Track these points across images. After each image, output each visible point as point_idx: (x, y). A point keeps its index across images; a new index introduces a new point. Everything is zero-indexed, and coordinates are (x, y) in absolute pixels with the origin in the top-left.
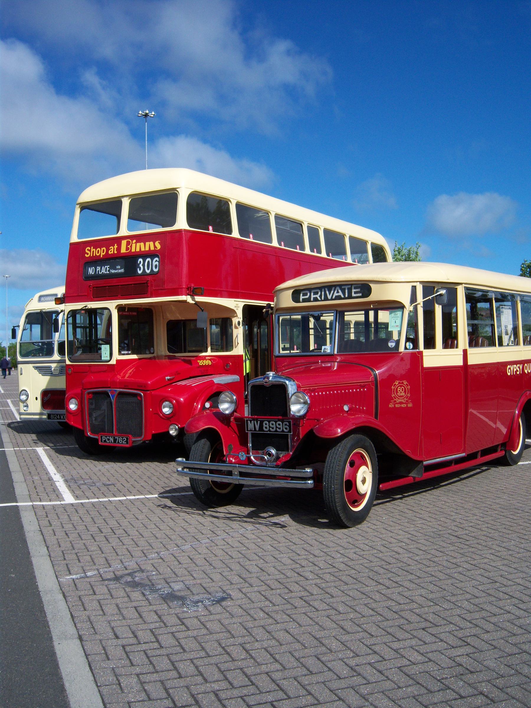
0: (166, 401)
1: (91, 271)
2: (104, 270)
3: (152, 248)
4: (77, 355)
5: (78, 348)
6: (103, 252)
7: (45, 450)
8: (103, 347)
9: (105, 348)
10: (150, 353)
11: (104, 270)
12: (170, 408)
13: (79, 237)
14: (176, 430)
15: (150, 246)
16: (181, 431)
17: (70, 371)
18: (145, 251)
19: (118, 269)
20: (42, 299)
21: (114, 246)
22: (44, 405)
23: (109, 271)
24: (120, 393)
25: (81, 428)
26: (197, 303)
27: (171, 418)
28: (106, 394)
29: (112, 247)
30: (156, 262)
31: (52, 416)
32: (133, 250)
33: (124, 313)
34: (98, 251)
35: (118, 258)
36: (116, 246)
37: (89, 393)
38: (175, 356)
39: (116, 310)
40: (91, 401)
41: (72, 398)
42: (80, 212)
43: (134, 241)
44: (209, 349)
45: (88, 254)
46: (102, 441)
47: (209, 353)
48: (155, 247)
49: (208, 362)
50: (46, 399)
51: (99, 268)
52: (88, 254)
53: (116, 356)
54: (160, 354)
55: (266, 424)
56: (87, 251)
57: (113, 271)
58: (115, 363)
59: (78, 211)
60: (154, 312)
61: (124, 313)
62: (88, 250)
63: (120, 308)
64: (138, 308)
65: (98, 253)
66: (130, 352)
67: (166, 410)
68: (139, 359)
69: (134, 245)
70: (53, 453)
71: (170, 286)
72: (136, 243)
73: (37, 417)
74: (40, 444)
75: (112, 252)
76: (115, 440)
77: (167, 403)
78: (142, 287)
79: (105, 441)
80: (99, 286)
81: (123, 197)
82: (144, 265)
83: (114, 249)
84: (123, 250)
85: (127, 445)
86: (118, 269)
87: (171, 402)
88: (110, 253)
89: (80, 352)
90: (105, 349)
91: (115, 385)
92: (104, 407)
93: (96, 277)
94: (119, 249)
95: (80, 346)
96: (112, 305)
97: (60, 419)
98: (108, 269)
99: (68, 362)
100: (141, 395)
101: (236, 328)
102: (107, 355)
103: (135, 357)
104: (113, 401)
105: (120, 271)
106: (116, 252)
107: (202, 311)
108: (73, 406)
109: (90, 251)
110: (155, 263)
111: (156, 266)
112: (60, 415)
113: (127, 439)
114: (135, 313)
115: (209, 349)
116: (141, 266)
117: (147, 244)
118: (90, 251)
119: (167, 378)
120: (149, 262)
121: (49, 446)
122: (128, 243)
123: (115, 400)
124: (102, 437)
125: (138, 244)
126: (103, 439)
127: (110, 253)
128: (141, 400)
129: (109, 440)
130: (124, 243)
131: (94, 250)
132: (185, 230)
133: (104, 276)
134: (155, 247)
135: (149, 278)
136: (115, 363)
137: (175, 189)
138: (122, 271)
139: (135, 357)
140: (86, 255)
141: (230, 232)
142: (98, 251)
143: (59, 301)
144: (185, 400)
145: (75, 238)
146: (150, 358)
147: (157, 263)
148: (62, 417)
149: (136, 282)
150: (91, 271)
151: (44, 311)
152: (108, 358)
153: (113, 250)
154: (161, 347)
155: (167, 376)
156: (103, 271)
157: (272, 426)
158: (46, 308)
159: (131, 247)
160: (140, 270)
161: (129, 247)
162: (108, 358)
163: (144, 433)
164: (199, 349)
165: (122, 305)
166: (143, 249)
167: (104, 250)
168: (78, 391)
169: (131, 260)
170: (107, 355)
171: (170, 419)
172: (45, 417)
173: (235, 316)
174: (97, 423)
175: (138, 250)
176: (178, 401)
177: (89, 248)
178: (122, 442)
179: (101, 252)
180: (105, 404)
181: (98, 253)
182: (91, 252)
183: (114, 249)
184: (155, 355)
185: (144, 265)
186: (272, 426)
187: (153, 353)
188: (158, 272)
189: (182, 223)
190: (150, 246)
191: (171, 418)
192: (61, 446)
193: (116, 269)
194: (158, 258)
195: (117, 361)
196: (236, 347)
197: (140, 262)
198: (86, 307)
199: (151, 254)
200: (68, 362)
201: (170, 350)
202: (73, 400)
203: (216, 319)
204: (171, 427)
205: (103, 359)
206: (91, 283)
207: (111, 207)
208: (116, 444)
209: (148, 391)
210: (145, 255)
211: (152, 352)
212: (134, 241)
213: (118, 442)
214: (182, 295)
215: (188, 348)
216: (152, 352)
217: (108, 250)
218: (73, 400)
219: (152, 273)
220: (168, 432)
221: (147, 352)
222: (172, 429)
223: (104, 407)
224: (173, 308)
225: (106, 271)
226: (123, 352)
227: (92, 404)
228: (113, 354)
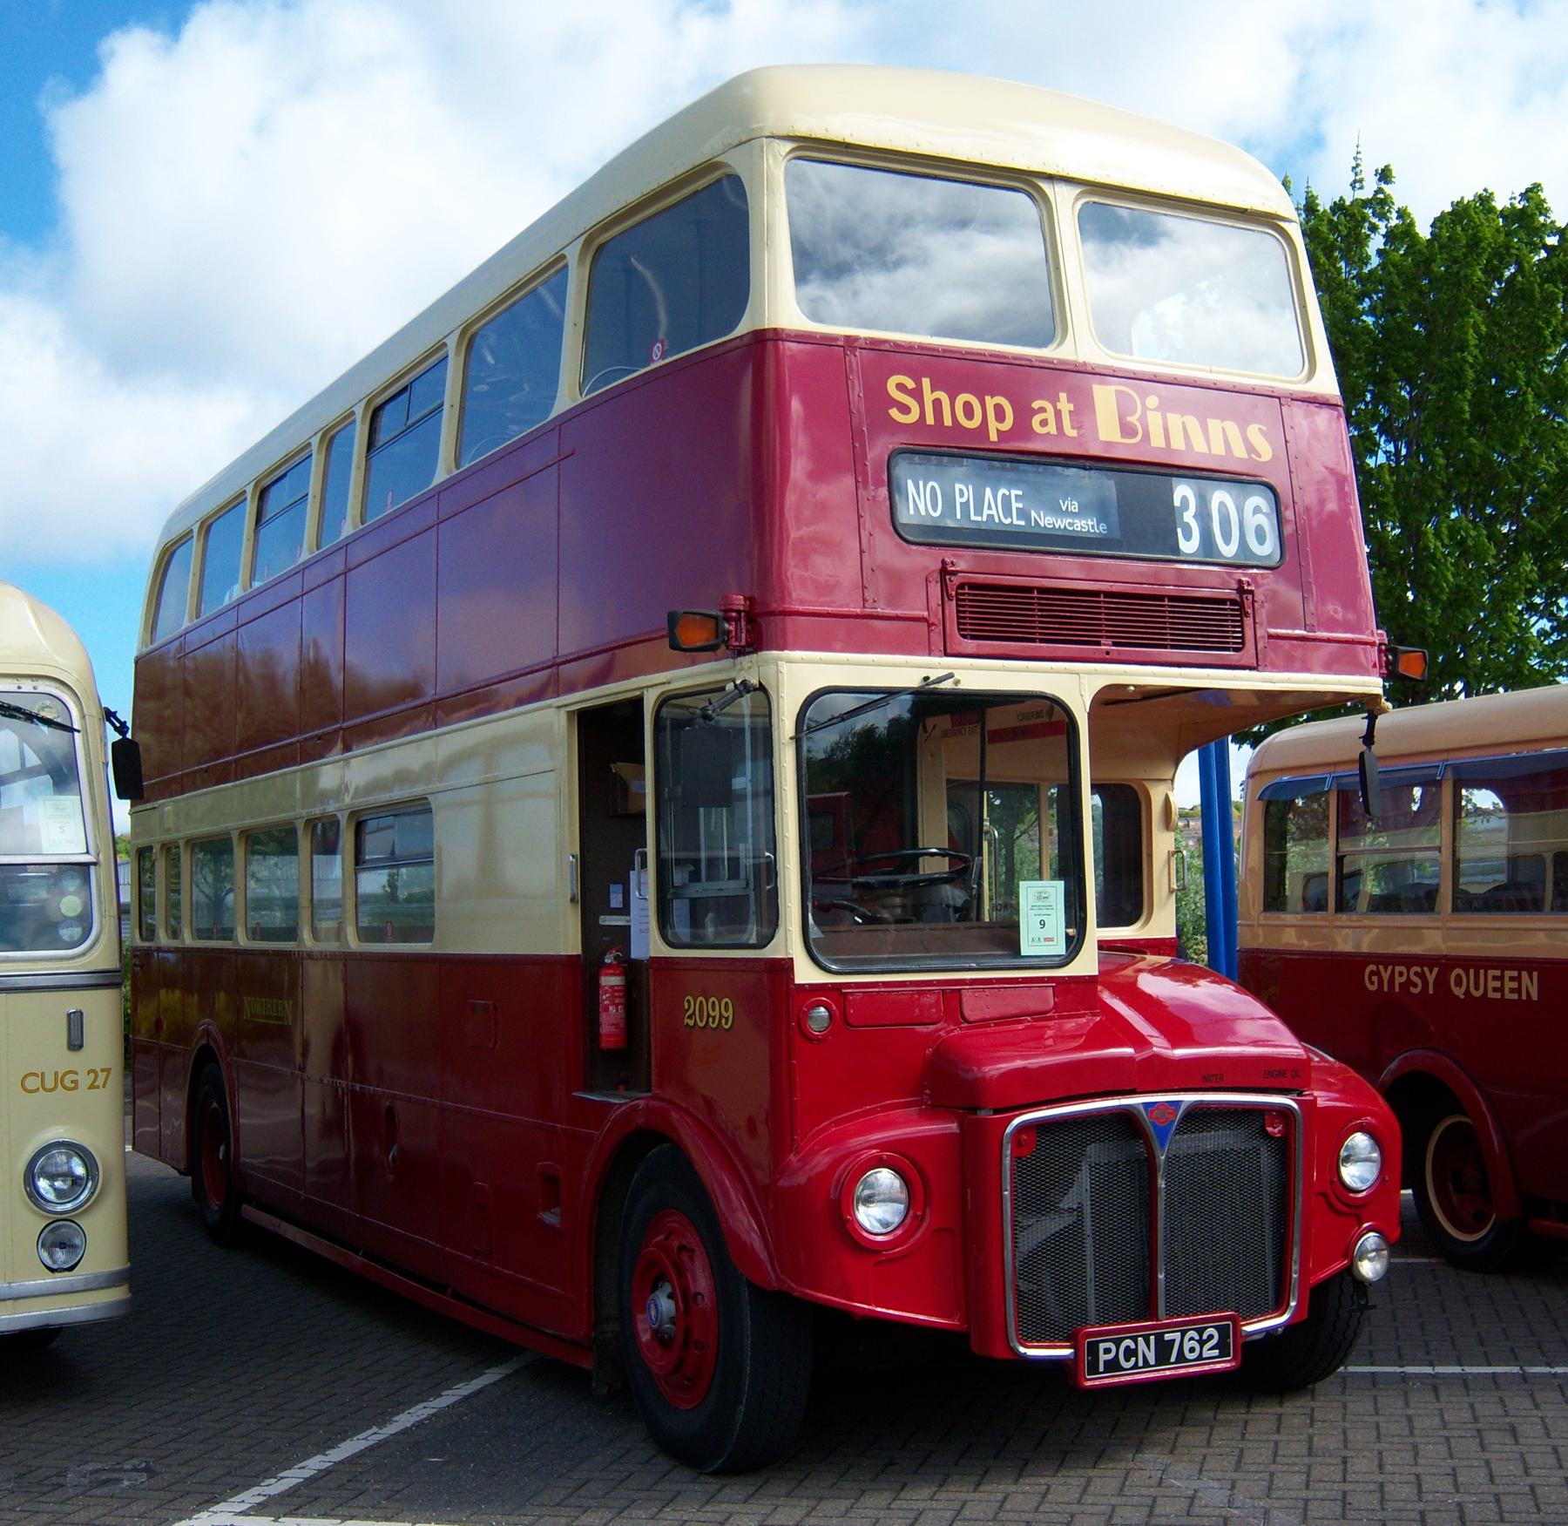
9: (1041, 897)
19: (1068, 513)
21: (1054, 401)
23: (1022, 514)
46: (1094, 1369)
52: (905, 409)
62: (901, 387)
76: (1163, 1351)
78: (1213, 621)
79: (1113, 1365)
80: (980, 578)
83: (1058, 414)
86: (1068, 513)
98: (1015, 505)
109: (917, 394)
116: (1189, 517)
118: (917, 394)
124: (1094, 1349)
126: (1103, 1357)
134: (1250, 448)
152: (1060, 948)
160: (1188, 537)
183: (1058, 414)
193: (1057, 511)
197: (1184, 500)
205: (1025, 950)
213: (1181, 1357)
225: (1007, 511)
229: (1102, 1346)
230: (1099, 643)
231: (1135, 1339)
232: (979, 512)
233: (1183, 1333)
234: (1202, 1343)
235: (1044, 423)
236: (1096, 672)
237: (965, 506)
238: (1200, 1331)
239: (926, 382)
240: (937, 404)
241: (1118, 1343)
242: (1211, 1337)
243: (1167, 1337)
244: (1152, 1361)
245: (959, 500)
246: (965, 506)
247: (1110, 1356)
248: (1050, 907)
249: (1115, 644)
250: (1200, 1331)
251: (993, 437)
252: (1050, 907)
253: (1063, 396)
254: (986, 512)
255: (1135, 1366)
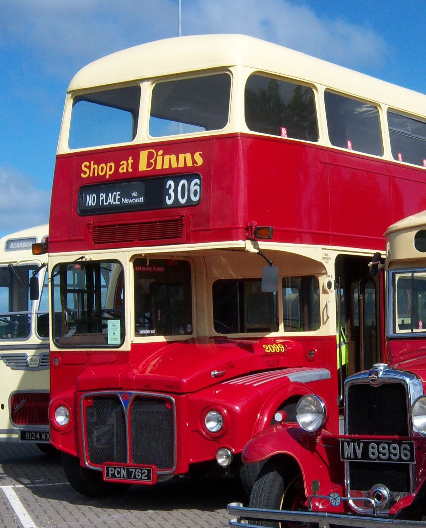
0: (212, 410)
1: (90, 200)
2: (112, 199)
3: (190, 164)
4: (68, 335)
5: (70, 325)
6: (110, 170)
7: (17, 490)
8: (110, 323)
9: (114, 325)
10: (187, 333)
11: (112, 199)
12: (218, 421)
13: (71, 146)
14: (228, 457)
15: (185, 160)
16: (236, 460)
17: (56, 363)
18: (178, 168)
19: (135, 197)
20: (12, 245)
21: (127, 160)
22: (15, 416)
23: (120, 200)
24: (138, 398)
25: (74, 453)
26: (262, 253)
27: (219, 437)
28: (115, 399)
29: (125, 162)
30: (195, 185)
31: (27, 435)
32: (159, 167)
33: (144, 269)
34: (102, 168)
35: (134, 179)
36: (131, 161)
37: (87, 398)
38: (226, 338)
39: (132, 264)
40: (90, 410)
41: (60, 405)
42: (74, 105)
43: (161, 152)
44: (281, 326)
45: (85, 173)
46: (108, 475)
47: (281, 332)
48: (194, 161)
49: (279, 348)
50: (17, 407)
51: (103, 196)
52: (85, 173)
53: (132, 338)
54: (201, 334)
55: (373, 449)
56: (84, 168)
57: (126, 201)
58: (129, 349)
59: (69, 103)
60: (192, 267)
61: (144, 269)
62: (86, 166)
63: (137, 261)
64: (166, 260)
65: (102, 171)
66: (153, 332)
67: (212, 426)
68: (168, 343)
69: (160, 159)
70: (29, 494)
71: (218, 224)
72: (163, 155)
73: (4, 436)
74: (8, 479)
75: (125, 170)
76: (129, 474)
77: (213, 413)
78: (173, 225)
81: (143, 80)
82: (175, 191)
83: (128, 164)
84: (143, 167)
85: (150, 482)
86: (135, 197)
87: (220, 412)
88: (121, 171)
89: (72, 332)
90: (113, 326)
91: (129, 384)
92: (112, 420)
93: (99, 210)
94: (136, 165)
95: (73, 321)
96: (124, 256)
97: (41, 439)
98: (118, 197)
99: (53, 348)
100: (171, 401)
101: (325, 292)
102: (116, 336)
103: (161, 339)
104: (126, 410)
105: (137, 200)
106: (130, 170)
107: (271, 264)
108: (61, 419)
109: (89, 168)
110: (193, 188)
111: (196, 192)
112: (40, 433)
113: (149, 471)
114: (161, 269)
115: (281, 326)
116: (171, 192)
117: (182, 156)
118: (89, 168)
119: (213, 373)
120: (183, 186)
121: (22, 483)
122: (150, 156)
123: (130, 409)
124: (108, 468)
125: (167, 157)
126: (110, 472)
127: (121, 171)
128: (172, 409)
129: (119, 473)
130: (144, 155)
131: (96, 166)
132: (242, 135)
133: (111, 209)
134: (194, 161)
135: (185, 212)
136: (129, 349)
137: (226, 68)
138: (141, 200)
139: (161, 339)
140: (83, 175)
141: (315, 136)
142: (102, 168)
143: (39, 249)
144: (242, 409)
145: (64, 148)
146: (186, 342)
147: (197, 188)
148: (44, 437)
149: (163, 219)
150: (90, 200)
151: (14, 264)
152: (119, 342)
153: (126, 167)
154: (204, 324)
155: (213, 370)
156: (111, 200)
157: (382, 451)
158: (18, 260)
159: (155, 161)
160: (170, 199)
161: (152, 161)
162: (119, 342)
163: (175, 463)
164: (264, 326)
165: (141, 255)
166: (174, 165)
167: (111, 167)
168: (70, 394)
169: (154, 182)
170: (116, 336)
171: (218, 440)
172: (16, 436)
173: (324, 274)
174: (100, 447)
175: (166, 166)
176: (231, 411)
177: (88, 164)
178: (140, 477)
179: (106, 170)
180: (114, 415)
181: (102, 171)
182: (89, 170)
183: (128, 164)
184: (194, 335)
185: (175, 191)
186: (382, 451)
187: (191, 333)
188: (199, 202)
189: (237, 123)
190: (185, 160)
191: (219, 437)
192: (42, 483)
193: (130, 197)
194: (200, 179)
195: (134, 346)
196: (324, 324)
197: (170, 186)
198: (82, 258)
199: (187, 174)
200: (53, 348)
201: (217, 328)
202: (62, 408)
203: (292, 277)
204: (220, 452)
206: (91, 220)
207: (123, 97)
208: (131, 481)
209: (183, 394)
210: (177, 175)
211: (189, 331)
212: (161, 152)
213: (135, 477)
214: (237, 239)
215: (247, 326)
216: (189, 331)
217: (118, 166)
218: (62, 410)
219: (190, 204)
220: (215, 461)
221: (181, 332)
222: (221, 456)
223: (112, 420)
224: (223, 260)
225: (115, 200)
226: (142, 332)
227: (92, 415)
228: (126, 334)
229: (110, 469)
230: (133, 241)
231: (120, 468)
232: (106, 202)
233: (136, 469)
234: (142, 474)
235: (123, 169)
236: (130, 251)
237: (103, 200)
238: (141, 470)
239: (92, 162)
240: (94, 169)
241: (115, 468)
242: (145, 472)
243: (130, 470)
244: (126, 477)
245: (101, 199)
246: (103, 200)
247: (113, 472)
248: (116, 328)
249: (139, 240)
250: (141, 470)
251: (107, 177)
252: (116, 328)
253: (130, 158)
254: (108, 201)
255: (120, 477)
